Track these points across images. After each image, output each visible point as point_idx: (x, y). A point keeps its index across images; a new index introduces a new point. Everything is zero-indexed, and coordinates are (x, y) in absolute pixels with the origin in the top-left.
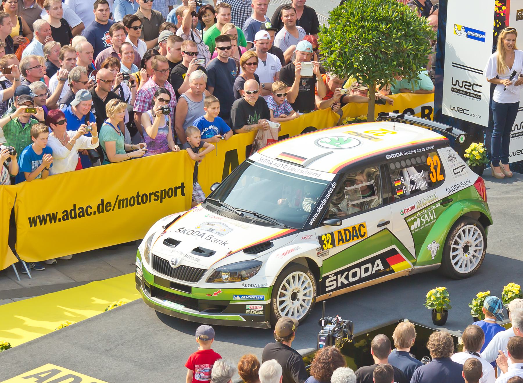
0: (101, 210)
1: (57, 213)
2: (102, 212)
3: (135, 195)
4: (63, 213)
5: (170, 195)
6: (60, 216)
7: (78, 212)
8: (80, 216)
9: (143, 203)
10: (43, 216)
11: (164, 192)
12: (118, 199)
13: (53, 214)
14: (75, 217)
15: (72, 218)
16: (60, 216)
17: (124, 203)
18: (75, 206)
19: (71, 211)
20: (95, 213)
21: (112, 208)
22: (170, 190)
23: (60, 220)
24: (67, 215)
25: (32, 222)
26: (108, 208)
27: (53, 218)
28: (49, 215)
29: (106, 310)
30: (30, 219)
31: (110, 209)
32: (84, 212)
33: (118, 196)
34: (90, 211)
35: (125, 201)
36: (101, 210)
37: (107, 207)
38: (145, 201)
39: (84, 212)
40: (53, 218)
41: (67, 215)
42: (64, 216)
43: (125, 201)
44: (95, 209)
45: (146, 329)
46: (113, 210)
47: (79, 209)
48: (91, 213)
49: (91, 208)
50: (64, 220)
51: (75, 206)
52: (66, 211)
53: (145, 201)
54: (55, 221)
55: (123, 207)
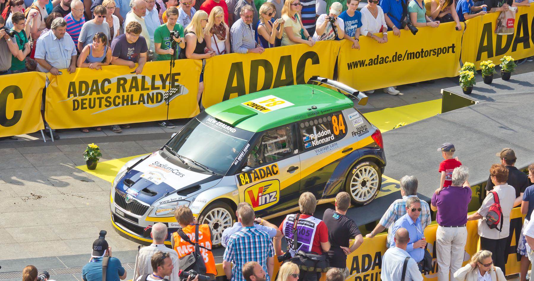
0: (394, 60)
1: (365, 60)
2: (396, 61)
3: (420, 51)
4: (370, 60)
5: (444, 52)
6: (367, 62)
7: (379, 60)
8: (380, 63)
9: (425, 56)
10: (356, 62)
11: (440, 50)
12: (407, 52)
13: (363, 61)
14: (377, 64)
15: (375, 64)
16: (367, 62)
17: (412, 56)
18: (378, 56)
19: (375, 59)
20: (390, 61)
21: (402, 58)
22: (445, 49)
23: (366, 65)
24: (372, 62)
25: (350, 66)
26: (400, 59)
27: (362, 63)
28: (360, 61)
29: (394, 128)
30: (348, 64)
31: (401, 59)
32: (384, 60)
33: (407, 51)
34: (387, 60)
35: (412, 54)
36: (394, 60)
37: (399, 57)
38: (426, 55)
39: (384, 60)
40: (362, 63)
41: (372, 62)
42: (370, 62)
43: (412, 54)
44: (391, 59)
45: (421, 142)
46: (403, 60)
47: (380, 59)
48: (388, 61)
49: (388, 58)
50: (369, 65)
51: (378, 56)
52: (372, 59)
53: (426, 55)
54: (363, 66)
55: (411, 58)
